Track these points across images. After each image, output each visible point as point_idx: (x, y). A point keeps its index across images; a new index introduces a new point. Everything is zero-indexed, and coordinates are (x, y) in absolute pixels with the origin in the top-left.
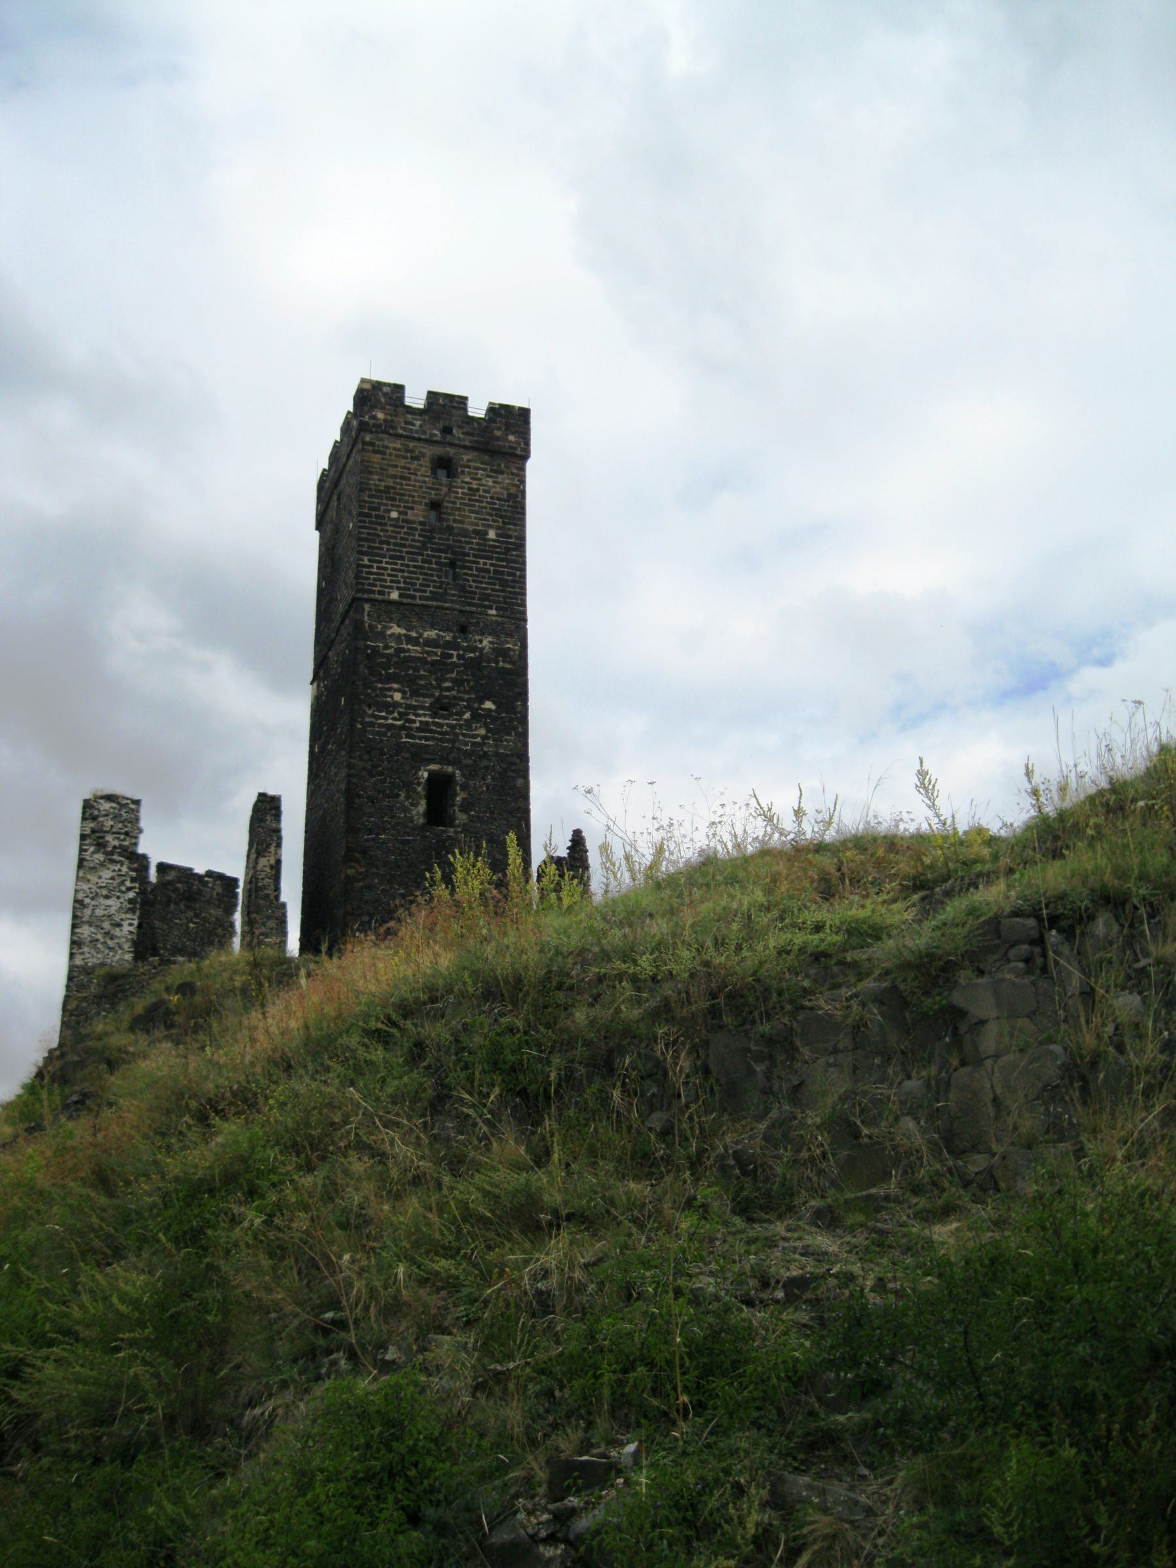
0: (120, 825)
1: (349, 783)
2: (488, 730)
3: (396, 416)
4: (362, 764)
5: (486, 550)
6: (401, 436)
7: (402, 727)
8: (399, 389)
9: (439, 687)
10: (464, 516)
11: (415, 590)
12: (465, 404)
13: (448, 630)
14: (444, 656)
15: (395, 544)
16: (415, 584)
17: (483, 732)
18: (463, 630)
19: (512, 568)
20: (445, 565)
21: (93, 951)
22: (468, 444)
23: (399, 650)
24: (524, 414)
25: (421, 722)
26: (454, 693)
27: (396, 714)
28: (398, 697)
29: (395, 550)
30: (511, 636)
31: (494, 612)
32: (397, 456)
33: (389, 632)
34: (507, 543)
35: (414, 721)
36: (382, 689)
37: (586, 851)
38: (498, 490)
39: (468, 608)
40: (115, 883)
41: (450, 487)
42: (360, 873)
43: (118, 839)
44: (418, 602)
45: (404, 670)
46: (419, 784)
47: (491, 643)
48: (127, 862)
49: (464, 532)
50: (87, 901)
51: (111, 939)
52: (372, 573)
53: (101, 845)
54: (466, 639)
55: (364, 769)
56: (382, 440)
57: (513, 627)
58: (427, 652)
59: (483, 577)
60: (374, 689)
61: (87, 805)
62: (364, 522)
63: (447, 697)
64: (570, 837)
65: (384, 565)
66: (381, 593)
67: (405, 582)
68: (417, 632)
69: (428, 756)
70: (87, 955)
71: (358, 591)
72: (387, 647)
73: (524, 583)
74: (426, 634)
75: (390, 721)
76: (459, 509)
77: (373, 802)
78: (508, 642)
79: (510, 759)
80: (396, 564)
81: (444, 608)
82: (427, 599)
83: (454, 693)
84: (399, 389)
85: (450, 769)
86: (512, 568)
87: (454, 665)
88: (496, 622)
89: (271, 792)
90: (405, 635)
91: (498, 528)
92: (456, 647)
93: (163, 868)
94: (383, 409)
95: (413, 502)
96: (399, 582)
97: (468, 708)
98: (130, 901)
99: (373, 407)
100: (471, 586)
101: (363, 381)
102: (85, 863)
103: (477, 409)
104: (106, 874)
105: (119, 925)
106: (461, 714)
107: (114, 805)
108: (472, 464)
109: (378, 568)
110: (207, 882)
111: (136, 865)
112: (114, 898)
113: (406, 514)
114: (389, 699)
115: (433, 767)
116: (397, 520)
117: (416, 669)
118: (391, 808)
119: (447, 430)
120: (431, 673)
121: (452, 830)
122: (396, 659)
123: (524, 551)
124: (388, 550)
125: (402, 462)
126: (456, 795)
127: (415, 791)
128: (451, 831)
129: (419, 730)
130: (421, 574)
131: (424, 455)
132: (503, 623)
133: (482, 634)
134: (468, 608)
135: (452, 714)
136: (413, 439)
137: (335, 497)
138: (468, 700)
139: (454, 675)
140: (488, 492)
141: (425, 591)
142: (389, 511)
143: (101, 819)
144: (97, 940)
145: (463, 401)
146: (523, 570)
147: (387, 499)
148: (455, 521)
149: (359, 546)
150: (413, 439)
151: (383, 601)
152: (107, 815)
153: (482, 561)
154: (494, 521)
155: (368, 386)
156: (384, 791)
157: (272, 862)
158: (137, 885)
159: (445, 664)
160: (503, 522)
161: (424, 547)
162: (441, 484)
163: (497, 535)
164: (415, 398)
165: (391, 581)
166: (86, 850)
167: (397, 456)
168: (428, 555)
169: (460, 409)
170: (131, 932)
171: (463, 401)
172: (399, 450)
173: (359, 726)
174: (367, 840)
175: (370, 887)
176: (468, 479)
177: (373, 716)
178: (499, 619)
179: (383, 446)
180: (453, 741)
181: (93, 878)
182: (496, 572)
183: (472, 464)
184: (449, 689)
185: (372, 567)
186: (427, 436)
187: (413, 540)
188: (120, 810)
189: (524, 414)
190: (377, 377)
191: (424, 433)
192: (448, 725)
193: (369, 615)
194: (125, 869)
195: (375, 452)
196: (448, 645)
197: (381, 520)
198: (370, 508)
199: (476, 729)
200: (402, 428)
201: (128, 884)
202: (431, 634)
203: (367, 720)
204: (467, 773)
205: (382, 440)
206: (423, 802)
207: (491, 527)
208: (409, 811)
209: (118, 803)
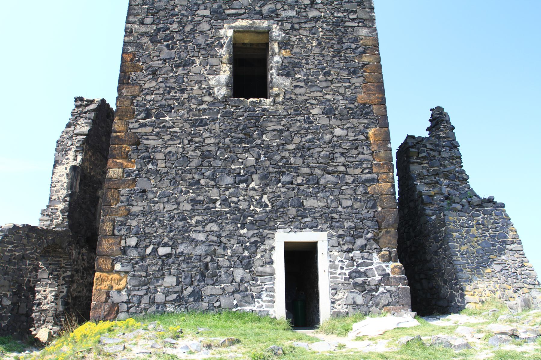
55: (143, 35)
77: (154, 73)
126: (274, 54)
128: (267, 102)
204: (288, 26)
208: (206, 80)
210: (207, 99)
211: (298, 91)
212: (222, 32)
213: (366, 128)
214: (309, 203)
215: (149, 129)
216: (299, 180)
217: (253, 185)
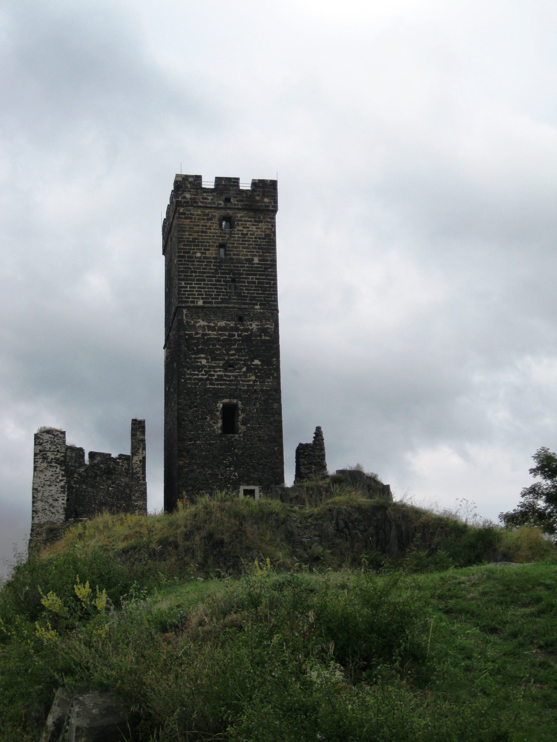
0: (55, 447)
1: (178, 413)
2: (257, 377)
3: (197, 195)
6: (200, 207)
7: (207, 379)
8: (198, 178)
10: (240, 251)
11: (212, 299)
12: (238, 183)
15: (199, 272)
17: (253, 378)
18: (241, 319)
19: (268, 279)
20: (228, 281)
21: (43, 515)
24: (274, 184)
25: (218, 375)
26: (237, 357)
27: (203, 372)
28: (204, 362)
29: (200, 276)
30: (269, 320)
32: (198, 219)
33: (198, 325)
34: (265, 264)
35: (214, 375)
36: (195, 358)
37: (323, 439)
38: (259, 233)
39: (243, 306)
40: (54, 478)
41: (231, 234)
42: (186, 463)
43: (54, 454)
45: (206, 346)
46: (218, 411)
47: (257, 325)
48: (59, 466)
49: (239, 261)
50: (39, 488)
51: (53, 508)
52: (187, 291)
53: (45, 458)
54: (242, 325)
57: (269, 315)
58: (221, 335)
59: (252, 287)
60: (191, 359)
61: (37, 437)
62: (181, 261)
63: (233, 359)
64: (314, 431)
65: (193, 285)
66: (193, 302)
67: (206, 295)
68: (214, 323)
69: (222, 395)
70: (41, 518)
71: (179, 302)
72: (197, 334)
73: (276, 288)
74: (219, 324)
75: (200, 376)
76: (237, 247)
77: (192, 423)
78: (267, 324)
80: (200, 284)
81: (229, 308)
82: (219, 303)
83: (237, 357)
84: (198, 178)
85: (235, 401)
86: (268, 279)
88: (260, 312)
89: (139, 418)
90: (207, 326)
91: (260, 256)
92: (237, 330)
93: (92, 455)
95: (209, 246)
96: (202, 295)
97: (244, 364)
98: (62, 487)
99: (184, 191)
100: (244, 293)
101: (177, 176)
102: (37, 469)
103: (245, 185)
104: (49, 473)
105: (57, 500)
106: (240, 369)
107: (51, 436)
108: (243, 219)
109: (190, 287)
110: (119, 462)
111: (64, 468)
112: (54, 486)
113: (205, 253)
114: (199, 364)
115: (226, 401)
116: (200, 258)
117: (214, 345)
118: (202, 426)
119: (227, 200)
120: (223, 346)
121: (237, 435)
123: (276, 268)
125: (202, 223)
126: (239, 415)
127: (215, 415)
129: (216, 380)
130: (215, 288)
131: (214, 216)
132: (264, 313)
133: (252, 321)
134: (243, 306)
135: (235, 369)
138: (245, 360)
141: (218, 299)
142: (195, 253)
144: (46, 509)
145: (236, 181)
146: (275, 280)
148: (234, 255)
149: (179, 275)
150: (208, 207)
151: (193, 307)
152: (47, 442)
153: (250, 277)
154: (257, 252)
155: (180, 179)
157: (141, 458)
158: (65, 478)
159: (231, 340)
160: (262, 252)
162: (225, 233)
163: (259, 261)
164: (208, 183)
165: (198, 295)
166: (37, 462)
167: (198, 219)
168: (219, 277)
171: (236, 181)
172: (200, 215)
173: (183, 381)
174: (190, 445)
175: (192, 471)
176: (241, 228)
177: (190, 374)
178: (262, 311)
179: (191, 214)
180: (237, 385)
181: (42, 476)
182: (259, 283)
183: (243, 219)
187: (210, 269)
188: (54, 438)
189: (274, 184)
190: (185, 172)
192: (233, 376)
193: (186, 315)
194: (58, 470)
195: (186, 218)
196: (232, 329)
199: (250, 376)
200: (201, 202)
201: (60, 478)
202: (222, 323)
203: (187, 376)
207: (255, 256)
208: (212, 427)
209: (53, 435)
210: (213, 434)
212: (218, 405)
213: (274, 447)
214: (252, 475)
216: (249, 467)
217: (232, 469)
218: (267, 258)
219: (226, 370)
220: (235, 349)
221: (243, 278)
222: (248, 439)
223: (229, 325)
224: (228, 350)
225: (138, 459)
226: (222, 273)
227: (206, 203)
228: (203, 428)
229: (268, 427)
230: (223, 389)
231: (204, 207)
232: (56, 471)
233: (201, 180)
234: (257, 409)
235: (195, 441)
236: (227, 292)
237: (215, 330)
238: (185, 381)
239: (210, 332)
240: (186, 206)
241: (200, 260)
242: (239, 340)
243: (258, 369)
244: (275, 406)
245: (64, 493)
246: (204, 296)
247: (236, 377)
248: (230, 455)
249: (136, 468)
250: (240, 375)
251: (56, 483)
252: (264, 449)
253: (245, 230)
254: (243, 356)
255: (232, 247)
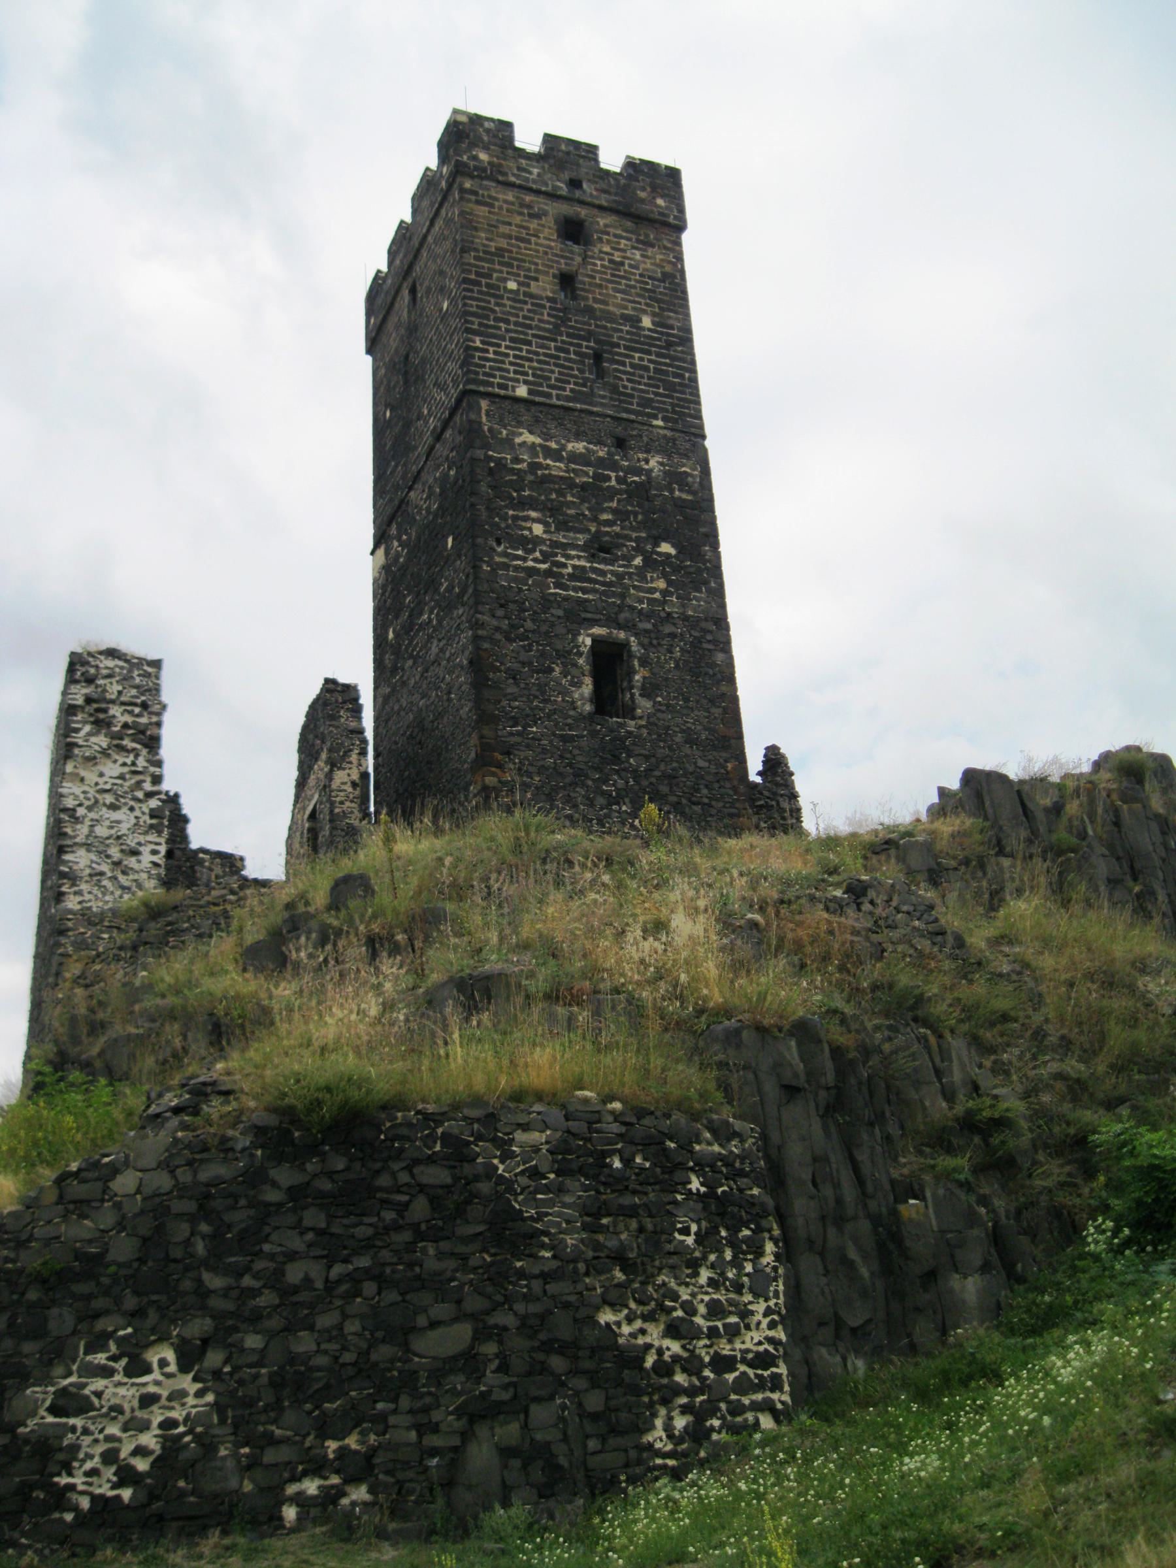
0: (134, 692)
1: (478, 648)
2: (670, 583)
4: (495, 623)
5: (638, 342)
7: (548, 573)
9: (595, 519)
10: (608, 295)
12: (596, 155)
13: (599, 443)
14: (596, 476)
15: (516, 324)
16: (549, 379)
21: (95, 890)
22: (604, 203)
23: (534, 466)
25: (574, 567)
27: (537, 554)
28: (538, 529)
29: (516, 332)
31: (660, 423)
33: (518, 440)
35: (565, 566)
43: (131, 713)
44: (554, 401)
46: (580, 654)
47: (661, 464)
48: (144, 752)
49: (610, 317)
51: (124, 873)
54: (625, 457)
55: (497, 629)
56: (487, 188)
58: (574, 470)
59: (642, 377)
60: (504, 518)
63: (608, 533)
65: (503, 350)
66: (501, 386)
67: (534, 375)
69: (589, 616)
70: (87, 897)
71: (468, 382)
73: (697, 388)
74: (570, 446)
75: (530, 564)
76: (600, 286)
79: (703, 624)
80: (521, 350)
81: (591, 413)
82: (568, 399)
83: (617, 529)
84: (507, 126)
85: (622, 635)
87: (613, 493)
91: (654, 315)
92: (615, 467)
94: (486, 148)
96: (526, 374)
97: (639, 550)
98: (153, 814)
99: (473, 145)
100: (625, 387)
102: (76, 751)
103: (611, 160)
104: (111, 770)
105: (135, 853)
106: (629, 559)
107: (121, 663)
108: (611, 230)
110: (203, 860)
112: (125, 809)
113: (528, 285)
114: (526, 533)
115: (598, 631)
117: (561, 493)
118: (542, 688)
119: (575, 184)
121: (633, 723)
122: (531, 478)
123: (692, 348)
124: (507, 331)
125: (517, 219)
126: (635, 672)
127: (575, 665)
128: (631, 725)
129: (572, 577)
130: (556, 365)
131: (545, 214)
132: (674, 440)
133: (648, 451)
134: (624, 415)
136: (530, 190)
137: (405, 293)
138: (638, 540)
139: (614, 504)
140: (637, 268)
141: (564, 389)
142: (505, 280)
143: (100, 682)
144: (102, 874)
146: (694, 371)
147: (500, 263)
148: (595, 300)
149: (467, 322)
150: (530, 190)
153: (637, 355)
154: (647, 305)
155: (463, 119)
156: (530, 663)
157: (355, 776)
159: (601, 489)
161: (556, 330)
163: (653, 323)
164: (528, 139)
165: (515, 372)
168: (563, 342)
169: (590, 159)
170: (156, 864)
171: (591, 151)
172: (512, 204)
174: (511, 734)
176: (607, 249)
177: (505, 554)
178: (669, 433)
181: (91, 776)
183: (611, 230)
184: (608, 523)
185: (487, 351)
186: (550, 188)
187: (540, 321)
191: (546, 185)
192: (613, 573)
193: (488, 415)
195: (478, 202)
196: (601, 463)
197: (496, 291)
198: (478, 274)
199: (652, 581)
202: (580, 446)
203: (497, 559)
204: (646, 641)
205: (487, 188)
206: (588, 681)
207: (645, 312)
208: (569, 693)
210: (572, 713)
211: (659, 715)
212: (580, 639)
215: (517, 739)
218: (671, 322)
219: (593, 556)
220: (614, 511)
221: (620, 354)
222: (659, 735)
223: (594, 452)
224: (597, 509)
225: (346, 779)
226: (568, 335)
227: (527, 179)
228: (543, 693)
229: (707, 710)
230: (587, 600)
231: (520, 187)
232: (134, 764)
233: (512, 132)
234: (677, 666)
235: (524, 728)
236: (586, 380)
237: (559, 459)
238: (493, 570)
239: (549, 462)
240: (479, 177)
241: (514, 296)
242: (619, 492)
243: (671, 565)
244: (720, 657)
245: (160, 833)
246: (530, 378)
247: (620, 577)
248: (617, 772)
249: (342, 803)
250: (630, 574)
251: (132, 803)
252: (701, 763)
253: (617, 253)
254: (632, 529)
255: (590, 284)
